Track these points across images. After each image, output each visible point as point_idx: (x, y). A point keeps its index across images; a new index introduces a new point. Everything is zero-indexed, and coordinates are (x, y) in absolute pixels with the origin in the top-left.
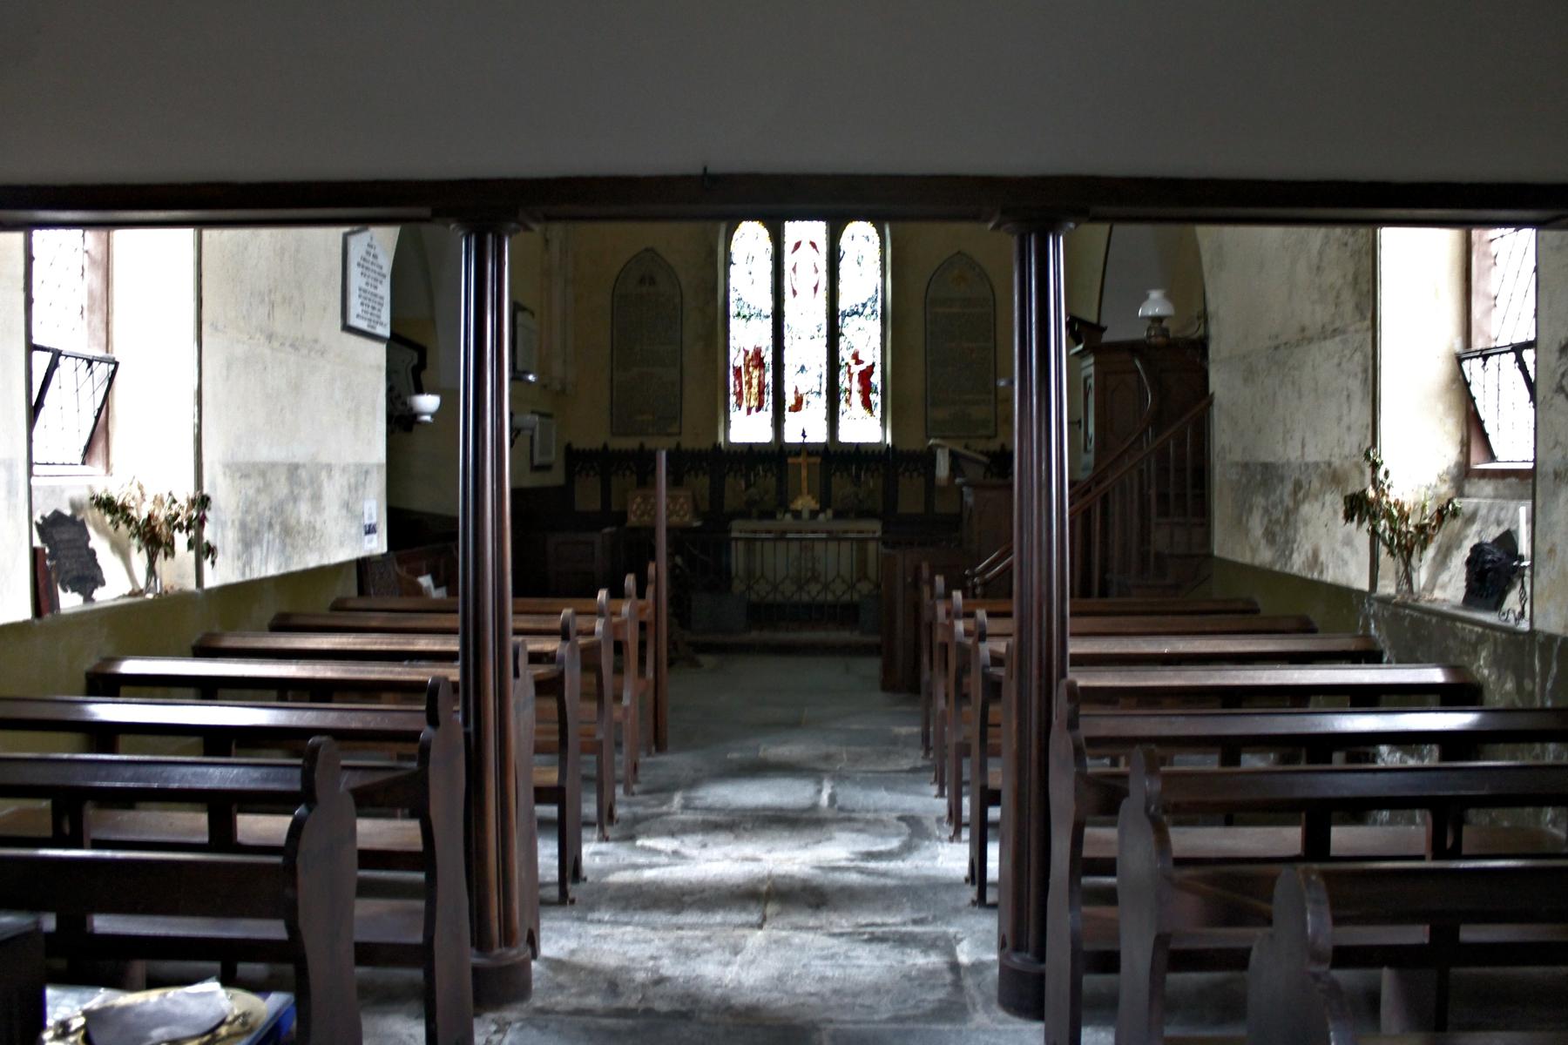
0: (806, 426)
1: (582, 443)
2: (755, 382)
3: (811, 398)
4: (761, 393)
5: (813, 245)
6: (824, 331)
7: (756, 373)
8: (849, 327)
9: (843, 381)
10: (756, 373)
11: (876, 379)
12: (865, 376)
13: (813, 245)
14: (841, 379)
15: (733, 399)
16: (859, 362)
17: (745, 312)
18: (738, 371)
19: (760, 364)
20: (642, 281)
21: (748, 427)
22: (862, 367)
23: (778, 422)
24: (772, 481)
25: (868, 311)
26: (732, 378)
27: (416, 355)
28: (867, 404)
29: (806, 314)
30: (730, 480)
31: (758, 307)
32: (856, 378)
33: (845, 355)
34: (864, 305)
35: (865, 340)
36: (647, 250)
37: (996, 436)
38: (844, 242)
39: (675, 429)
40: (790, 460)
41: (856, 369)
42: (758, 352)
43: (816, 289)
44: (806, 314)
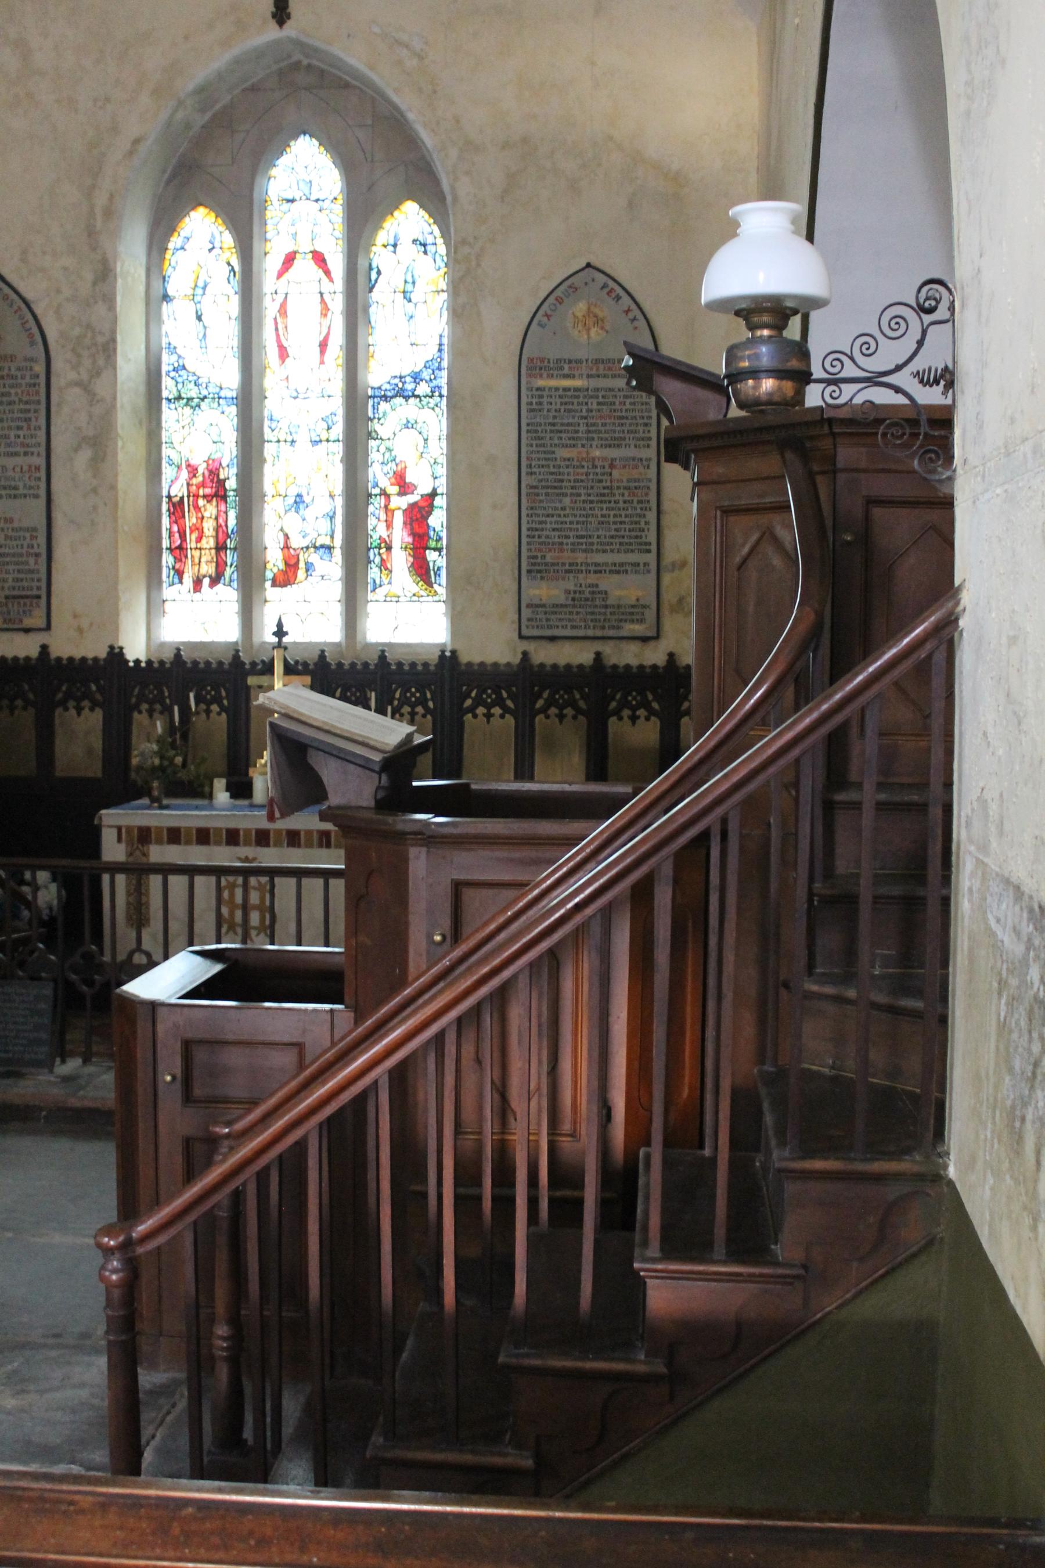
2: (209, 526)
3: (314, 557)
5: (319, 259)
6: (338, 430)
7: (210, 510)
8: (390, 420)
9: (376, 528)
12: (417, 517)
13: (319, 259)
14: (372, 522)
15: (167, 559)
16: (405, 488)
17: (193, 392)
19: (220, 494)
25: (423, 389)
26: (165, 521)
28: (421, 570)
29: (303, 398)
30: (140, 719)
31: (216, 380)
32: (399, 519)
33: (379, 475)
34: (416, 378)
35: (416, 446)
37: (657, 637)
38: (380, 256)
39: (37, 620)
42: (213, 472)
43: (323, 346)
44: (303, 398)
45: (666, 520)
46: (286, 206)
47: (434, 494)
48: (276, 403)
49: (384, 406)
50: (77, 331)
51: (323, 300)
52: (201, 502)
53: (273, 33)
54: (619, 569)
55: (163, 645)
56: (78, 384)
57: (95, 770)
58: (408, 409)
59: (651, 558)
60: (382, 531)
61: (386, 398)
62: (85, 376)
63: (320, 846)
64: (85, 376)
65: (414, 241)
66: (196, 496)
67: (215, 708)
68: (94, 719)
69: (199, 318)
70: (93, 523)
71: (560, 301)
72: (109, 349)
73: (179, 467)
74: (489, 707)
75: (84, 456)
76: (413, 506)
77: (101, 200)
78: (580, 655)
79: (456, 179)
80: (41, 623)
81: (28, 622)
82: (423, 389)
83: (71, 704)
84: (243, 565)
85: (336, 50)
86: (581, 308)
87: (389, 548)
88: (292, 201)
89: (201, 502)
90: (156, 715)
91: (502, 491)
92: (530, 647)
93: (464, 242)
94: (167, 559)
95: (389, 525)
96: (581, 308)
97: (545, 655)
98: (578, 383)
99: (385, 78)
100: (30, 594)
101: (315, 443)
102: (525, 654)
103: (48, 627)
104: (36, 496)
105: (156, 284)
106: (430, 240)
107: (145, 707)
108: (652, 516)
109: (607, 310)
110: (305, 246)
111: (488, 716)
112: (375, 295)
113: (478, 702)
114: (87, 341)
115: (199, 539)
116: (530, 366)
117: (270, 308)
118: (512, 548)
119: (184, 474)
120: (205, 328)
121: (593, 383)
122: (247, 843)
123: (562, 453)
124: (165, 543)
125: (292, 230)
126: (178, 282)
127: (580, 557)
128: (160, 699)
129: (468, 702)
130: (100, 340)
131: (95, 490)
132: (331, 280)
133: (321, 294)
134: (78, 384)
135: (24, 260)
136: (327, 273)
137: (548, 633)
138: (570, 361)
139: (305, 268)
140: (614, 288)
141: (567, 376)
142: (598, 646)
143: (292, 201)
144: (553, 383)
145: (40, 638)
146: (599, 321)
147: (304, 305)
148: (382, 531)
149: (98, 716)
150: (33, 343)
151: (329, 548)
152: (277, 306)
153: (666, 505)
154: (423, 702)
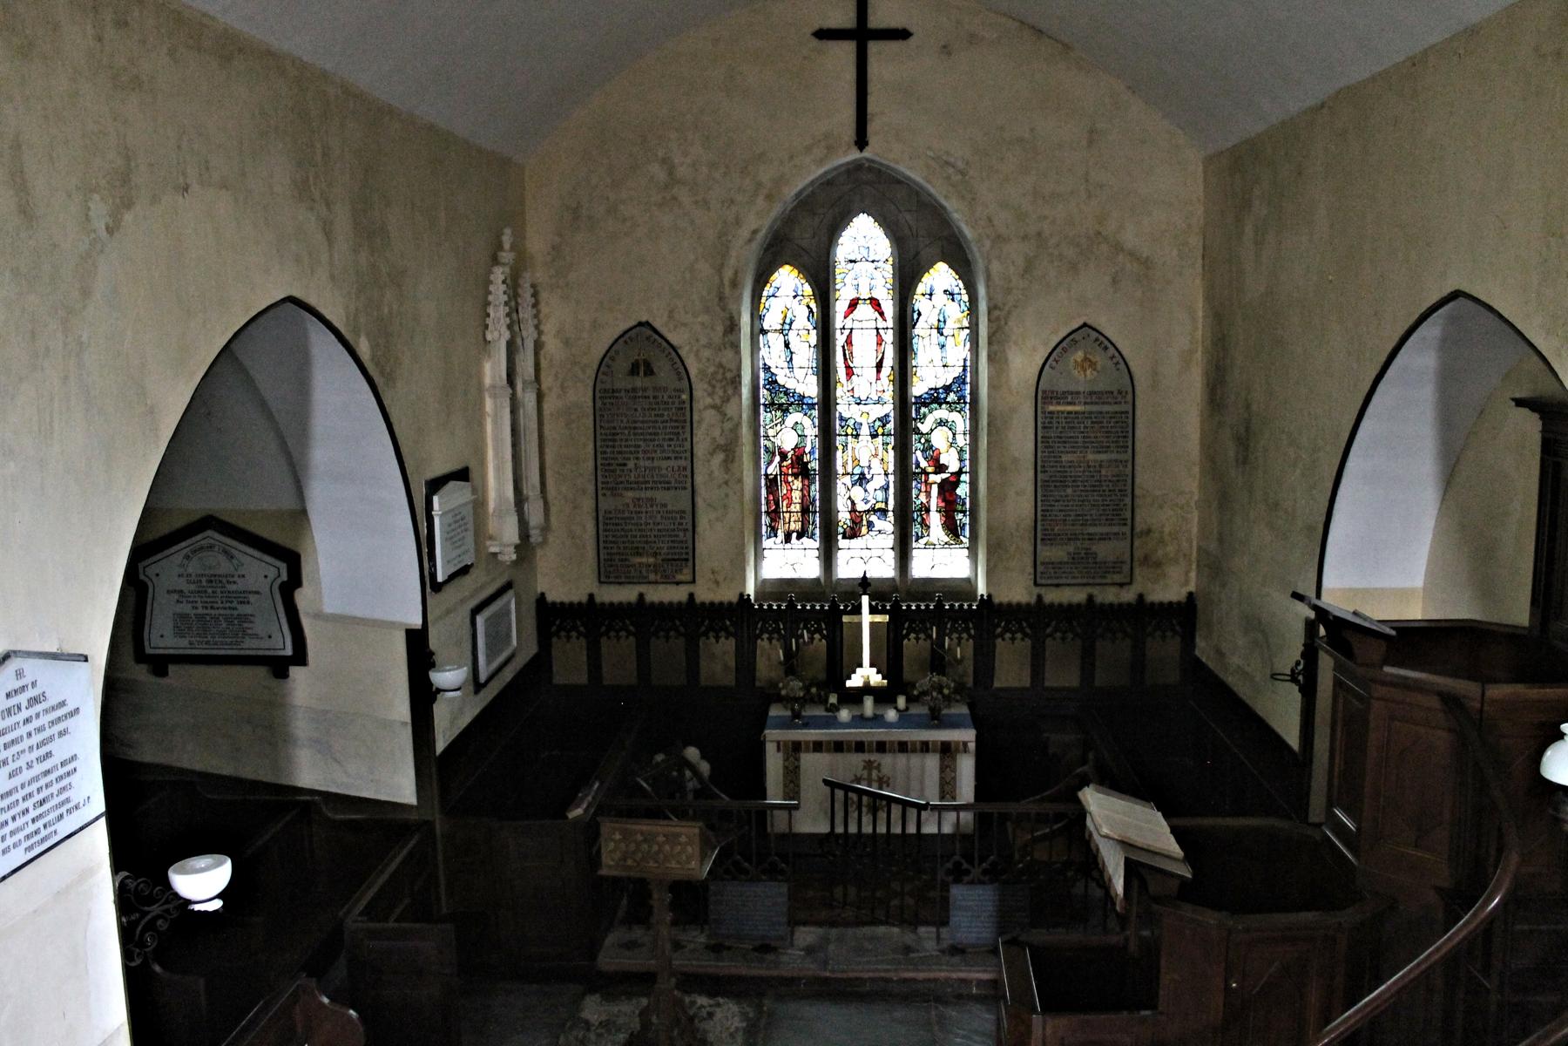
0: (867, 557)
1: (556, 595)
2: (796, 495)
3: (873, 518)
4: (805, 511)
5: (875, 303)
7: (797, 484)
10: (797, 484)
12: (947, 488)
13: (875, 303)
15: (765, 519)
16: (940, 468)
18: (772, 483)
19: (802, 471)
20: (634, 370)
21: (788, 560)
23: (828, 555)
24: (820, 644)
27: (283, 567)
28: (952, 528)
30: (763, 644)
32: (935, 490)
34: (947, 389)
35: (946, 437)
36: (640, 324)
37: (1130, 583)
38: (920, 303)
39: (685, 575)
40: (845, 619)
41: (938, 478)
43: (879, 366)
45: (1138, 502)
47: (960, 472)
48: (844, 408)
49: (923, 410)
50: (712, 369)
53: (855, 155)
54: (1104, 538)
55: (765, 581)
56: (714, 407)
57: (729, 680)
58: (942, 413)
59: (1127, 530)
60: (923, 498)
61: (926, 405)
62: (718, 401)
64: (718, 401)
67: (817, 636)
69: (787, 345)
70: (725, 506)
72: (736, 381)
73: (773, 454)
74: (1013, 633)
75: (720, 456)
76: (943, 480)
77: (728, 274)
78: (1077, 596)
79: (990, 261)
80: (689, 578)
81: (679, 577)
82: (952, 397)
83: (711, 634)
85: (901, 168)
86: (1079, 355)
87: (928, 511)
92: (1043, 591)
94: (765, 519)
95: (928, 494)
96: (1079, 355)
97: (1052, 596)
98: (1077, 408)
99: (937, 190)
101: (874, 436)
102: (1040, 597)
103: (694, 581)
105: (757, 322)
106: (956, 290)
107: (765, 636)
108: (1128, 500)
109: (1100, 358)
110: (865, 294)
111: (1013, 639)
112: (916, 331)
113: (1006, 630)
114: (720, 377)
115: (789, 506)
116: (1043, 396)
117: (840, 339)
118: (1029, 522)
119: (777, 459)
121: (1088, 408)
122: (870, 751)
123: (1065, 458)
124: (764, 508)
126: (772, 320)
127: (1078, 529)
128: (777, 630)
130: (729, 375)
134: (714, 407)
135: (671, 317)
136: (882, 314)
139: (864, 311)
140: (1104, 342)
142: (1089, 590)
145: (690, 588)
146: (1093, 365)
147: (865, 337)
149: (732, 641)
150: (680, 379)
151: (884, 512)
152: (844, 338)
153: (1137, 492)
154: (967, 630)
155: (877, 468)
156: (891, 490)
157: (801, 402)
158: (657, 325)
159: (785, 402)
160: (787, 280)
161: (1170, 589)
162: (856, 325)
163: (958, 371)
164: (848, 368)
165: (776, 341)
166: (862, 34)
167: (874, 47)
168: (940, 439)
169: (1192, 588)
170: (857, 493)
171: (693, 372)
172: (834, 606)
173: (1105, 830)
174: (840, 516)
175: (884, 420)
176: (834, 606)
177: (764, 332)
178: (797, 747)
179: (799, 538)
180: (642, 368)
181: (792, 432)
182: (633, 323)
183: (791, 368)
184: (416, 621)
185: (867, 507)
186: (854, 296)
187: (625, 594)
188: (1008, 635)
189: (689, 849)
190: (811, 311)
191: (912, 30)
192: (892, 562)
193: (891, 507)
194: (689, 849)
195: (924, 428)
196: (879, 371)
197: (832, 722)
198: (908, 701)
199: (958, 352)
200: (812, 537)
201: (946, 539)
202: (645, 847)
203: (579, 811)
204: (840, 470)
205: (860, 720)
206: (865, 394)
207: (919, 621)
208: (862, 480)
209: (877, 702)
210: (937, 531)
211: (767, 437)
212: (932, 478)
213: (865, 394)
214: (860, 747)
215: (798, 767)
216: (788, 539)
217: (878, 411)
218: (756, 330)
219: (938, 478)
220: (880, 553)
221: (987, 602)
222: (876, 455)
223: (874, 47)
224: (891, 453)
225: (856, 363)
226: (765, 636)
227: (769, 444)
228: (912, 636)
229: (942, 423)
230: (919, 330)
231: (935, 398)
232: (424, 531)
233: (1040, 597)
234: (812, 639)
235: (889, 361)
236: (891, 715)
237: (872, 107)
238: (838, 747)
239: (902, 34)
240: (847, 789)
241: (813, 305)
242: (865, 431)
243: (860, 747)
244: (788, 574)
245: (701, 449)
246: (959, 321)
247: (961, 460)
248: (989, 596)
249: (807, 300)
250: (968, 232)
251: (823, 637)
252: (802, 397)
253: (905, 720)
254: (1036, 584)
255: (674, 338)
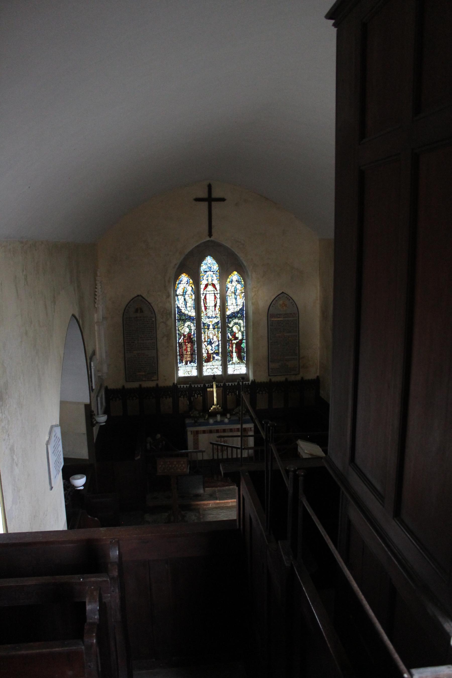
0: (212, 369)
2: (189, 349)
3: (215, 355)
4: (192, 355)
5: (214, 285)
7: (189, 345)
10: (189, 345)
11: (243, 345)
12: (239, 345)
13: (214, 285)
16: (236, 338)
18: (180, 344)
21: (186, 370)
22: (237, 341)
23: (200, 369)
28: (240, 357)
30: (181, 399)
32: (234, 346)
34: (238, 312)
35: (238, 329)
36: (138, 296)
37: (299, 374)
43: (215, 306)
46: (205, 273)
47: (242, 339)
48: (205, 320)
49: (230, 319)
51: (215, 296)
52: (187, 344)
53: (208, 239)
56: (163, 322)
58: (236, 321)
60: (230, 349)
61: (231, 318)
63: (237, 431)
65: (236, 281)
66: (186, 342)
68: (170, 400)
69: (185, 299)
71: (276, 301)
75: (165, 338)
78: (282, 379)
81: (153, 379)
82: (239, 315)
84: (200, 360)
86: (281, 302)
87: (232, 352)
88: (206, 272)
89: (187, 344)
90: (185, 398)
91: (264, 344)
93: (254, 287)
97: (274, 379)
99: (235, 250)
100: (153, 371)
101: (214, 329)
102: (270, 380)
103: (158, 380)
104: (154, 349)
106: (240, 280)
107: (182, 396)
108: (297, 348)
112: (227, 294)
115: (186, 352)
116: (270, 315)
117: (203, 297)
119: (182, 337)
120: (186, 302)
122: (221, 432)
125: (207, 278)
126: (179, 291)
129: (258, 391)
131: (168, 347)
132: (217, 290)
133: (214, 294)
134: (163, 322)
136: (216, 289)
137: (275, 374)
138: (279, 314)
139: (210, 288)
140: (289, 298)
141: (278, 318)
143: (206, 272)
144: (276, 319)
148: (230, 349)
149: (171, 398)
155: (215, 339)
156: (220, 346)
157: (190, 318)
158: (143, 296)
159: (184, 318)
160: (184, 278)
161: (311, 375)
162: (207, 292)
163: (241, 307)
164: (205, 306)
165: (181, 298)
166: (210, 200)
167: (213, 204)
168: (235, 329)
169: (318, 374)
170: (209, 347)
171: (156, 311)
172: (204, 385)
173: (306, 451)
174: (204, 355)
175: (217, 323)
176: (204, 385)
177: (177, 296)
178: (197, 432)
179: (190, 363)
180: (139, 310)
181: (186, 328)
182: (136, 295)
183: (186, 307)
184: (87, 401)
185: (212, 352)
186: (206, 282)
187: (135, 385)
188: (261, 392)
189: (184, 465)
190: (192, 288)
191: (226, 198)
192: (221, 370)
193: (220, 352)
194: (184, 465)
195: (231, 325)
196: (215, 308)
197: (208, 424)
198: (231, 415)
199: (241, 301)
200: (194, 362)
201: (238, 361)
202: (170, 466)
203: (139, 457)
204: (203, 340)
205: (216, 423)
206: (211, 315)
207: (233, 389)
208: (210, 343)
209: (221, 416)
210: (235, 359)
211: (179, 330)
212: (233, 341)
213: (211, 315)
214: (217, 431)
215: (198, 439)
216: (186, 364)
217: (215, 320)
218: (175, 295)
219: (235, 342)
220: (217, 367)
221: (253, 382)
222: (215, 335)
223: (213, 204)
224: (220, 334)
225: (208, 305)
226: (182, 396)
227: (179, 332)
228: (230, 394)
229: (236, 324)
230: (229, 293)
231: (234, 315)
232: (89, 373)
233: (270, 380)
234: (197, 396)
235: (218, 304)
236: (226, 420)
237: (213, 223)
238: (211, 432)
239: (223, 200)
240: (218, 445)
241: (193, 286)
242: (211, 327)
243: (217, 431)
244: (187, 375)
245: (159, 336)
246: (241, 290)
247: (243, 335)
248: (254, 380)
249: (191, 285)
250: (245, 264)
251: (201, 396)
252: (190, 317)
253: (231, 422)
254: (269, 375)
255: (149, 300)
